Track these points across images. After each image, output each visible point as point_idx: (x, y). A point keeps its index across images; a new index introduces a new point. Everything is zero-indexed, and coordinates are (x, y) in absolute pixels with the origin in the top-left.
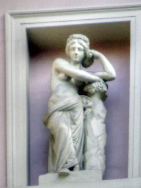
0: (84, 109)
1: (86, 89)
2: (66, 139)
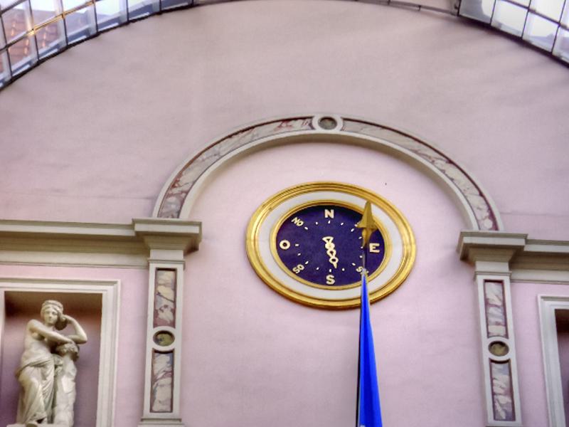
0: (56, 367)
1: (58, 349)
2: (36, 393)
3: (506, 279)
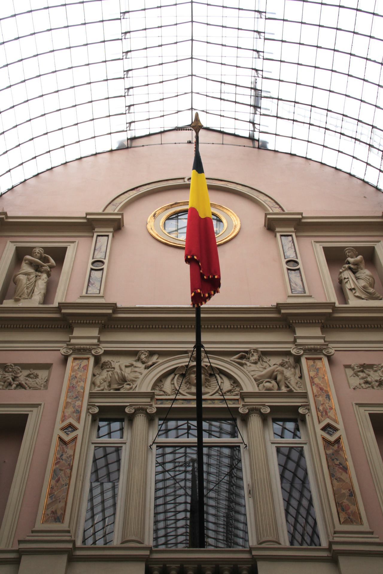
3: (294, 235)
